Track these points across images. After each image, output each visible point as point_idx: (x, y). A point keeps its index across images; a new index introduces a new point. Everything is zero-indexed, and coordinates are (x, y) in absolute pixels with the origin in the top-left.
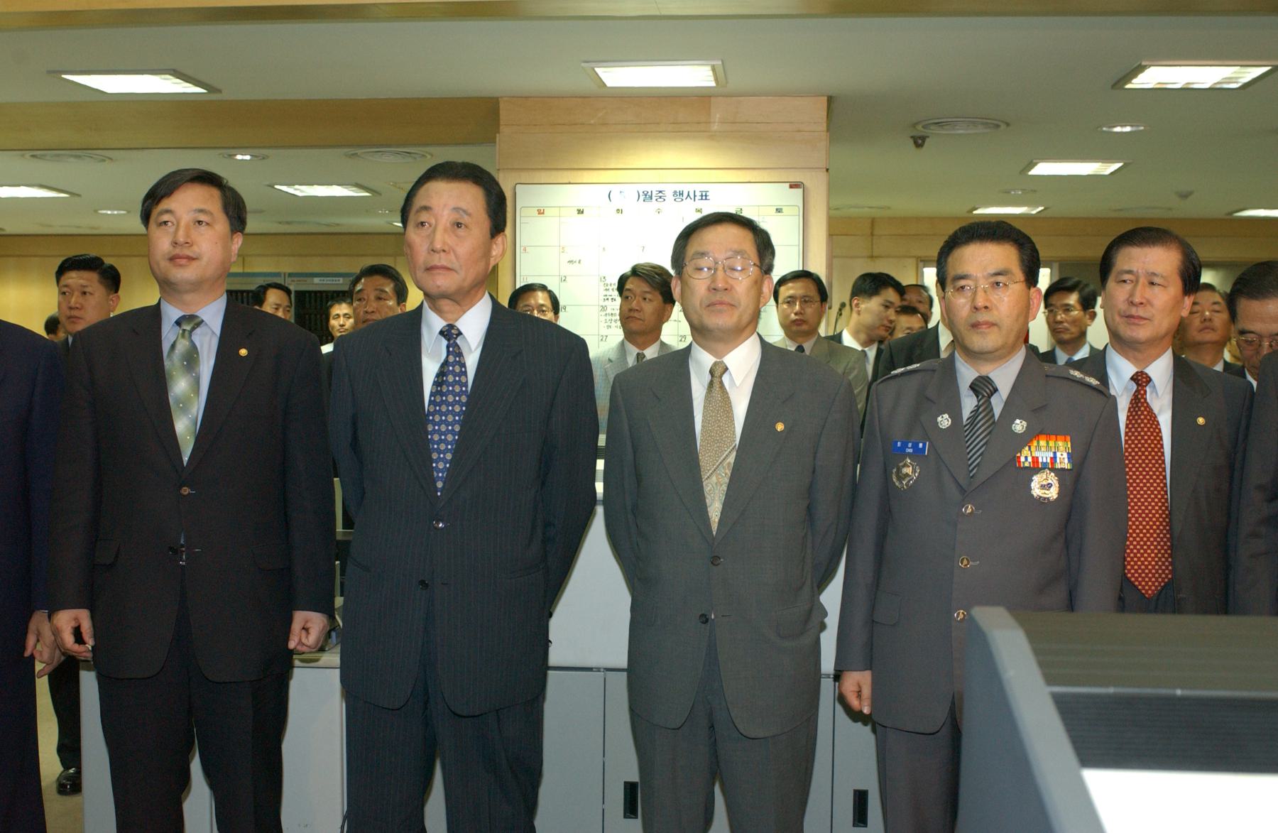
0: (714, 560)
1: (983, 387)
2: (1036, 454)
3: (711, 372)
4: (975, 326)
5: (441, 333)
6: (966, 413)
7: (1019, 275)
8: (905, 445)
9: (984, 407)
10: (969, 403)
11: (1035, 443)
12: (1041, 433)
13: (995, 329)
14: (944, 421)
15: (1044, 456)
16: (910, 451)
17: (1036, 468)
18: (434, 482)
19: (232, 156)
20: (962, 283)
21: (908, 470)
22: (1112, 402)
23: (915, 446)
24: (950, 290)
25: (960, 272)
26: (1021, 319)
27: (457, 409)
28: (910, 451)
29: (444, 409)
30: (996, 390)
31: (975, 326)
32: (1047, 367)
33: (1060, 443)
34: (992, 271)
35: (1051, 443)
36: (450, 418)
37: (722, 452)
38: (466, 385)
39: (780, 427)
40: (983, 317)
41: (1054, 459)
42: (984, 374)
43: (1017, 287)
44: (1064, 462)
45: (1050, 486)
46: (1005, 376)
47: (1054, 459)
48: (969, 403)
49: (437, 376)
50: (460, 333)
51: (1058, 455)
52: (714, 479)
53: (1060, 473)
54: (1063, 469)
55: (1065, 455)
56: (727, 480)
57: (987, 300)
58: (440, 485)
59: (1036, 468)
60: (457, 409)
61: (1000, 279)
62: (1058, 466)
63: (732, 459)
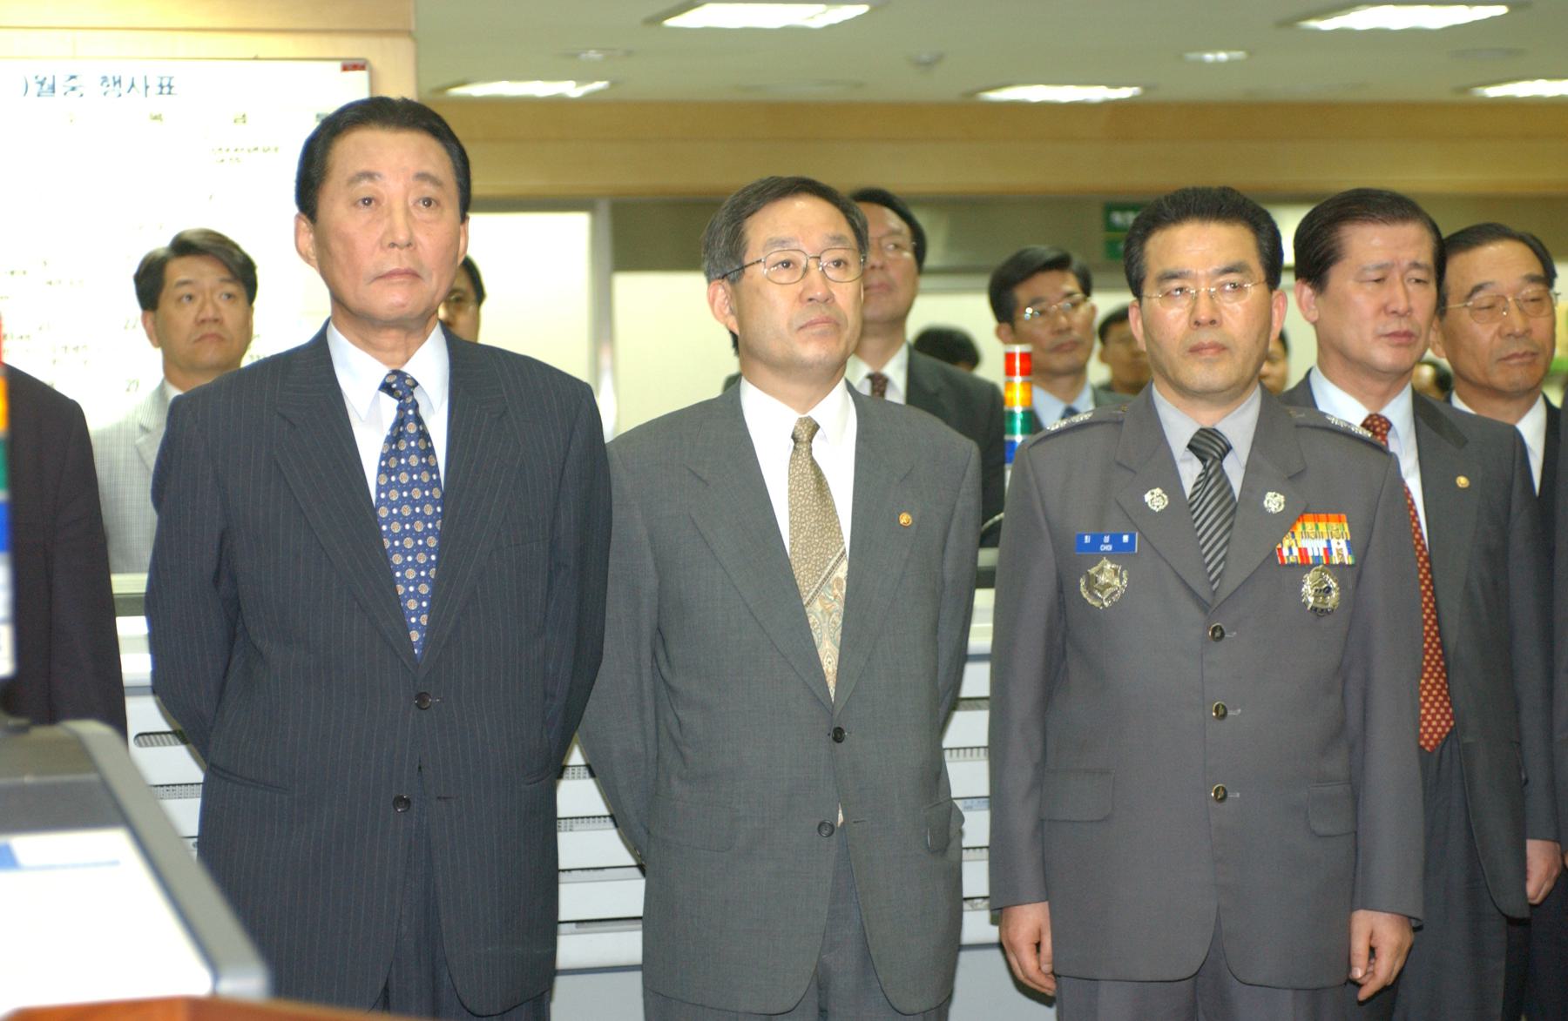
0: (838, 735)
1: (1208, 445)
3: (794, 437)
4: (1196, 350)
5: (386, 387)
6: (1188, 490)
7: (1259, 272)
8: (1097, 540)
9: (1213, 476)
10: (1190, 471)
12: (1306, 511)
13: (1226, 355)
14: (1156, 500)
16: (1109, 548)
18: (406, 629)
19: (613, 84)
20: (1176, 284)
21: (1103, 579)
22: (1392, 461)
23: (1116, 540)
24: (1151, 292)
25: (1171, 265)
26: (1263, 340)
27: (429, 510)
28: (1109, 548)
29: (406, 511)
30: (1229, 448)
31: (1196, 350)
32: (1299, 415)
33: (1334, 526)
34: (1223, 266)
36: (419, 526)
37: (825, 563)
38: (435, 470)
39: (905, 519)
40: (1207, 336)
41: (1328, 550)
42: (1207, 425)
43: (1254, 291)
44: (1342, 553)
45: (1328, 590)
46: (1239, 425)
47: (1328, 550)
48: (1190, 471)
49: (384, 457)
50: (416, 384)
51: (1334, 542)
52: (817, 606)
54: (1342, 565)
56: (839, 606)
57: (1215, 309)
58: (415, 636)
60: (429, 510)
61: (1234, 277)
63: (842, 571)
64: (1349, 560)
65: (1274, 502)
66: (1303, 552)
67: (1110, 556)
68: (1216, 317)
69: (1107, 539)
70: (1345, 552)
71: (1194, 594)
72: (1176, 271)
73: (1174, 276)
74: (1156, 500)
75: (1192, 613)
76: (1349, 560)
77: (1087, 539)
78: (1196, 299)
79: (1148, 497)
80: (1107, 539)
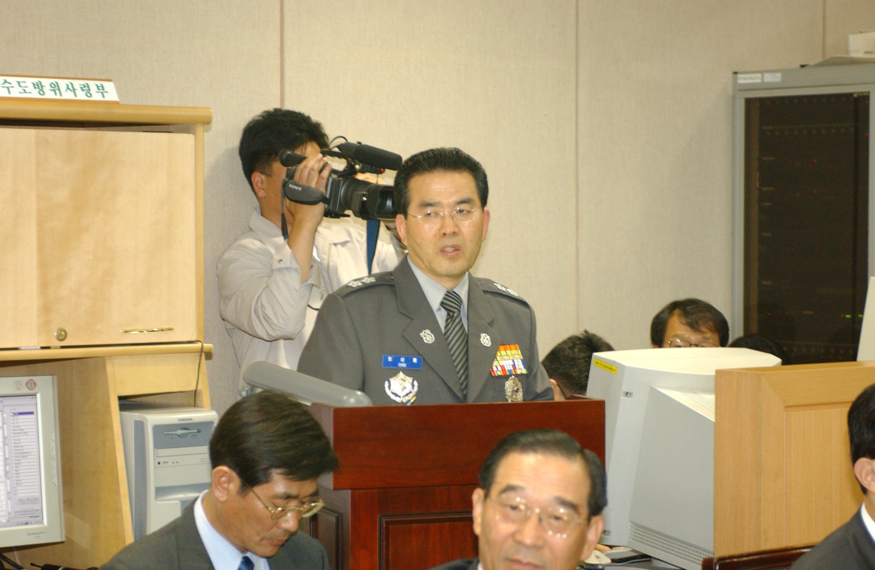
2: (502, 363)
8: (396, 361)
11: (499, 354)
14: (428, 337)
15: (508, 365)
16: (404, 365)
17: (506, 377)
23: (408, 361)
28: (404, 365)
33: (514, 352)
35: (509, 352)
41: (514, 366)
45: (517, 391)
51: (516, 361)
54: (522, 375)
55: (520, 362)
57: (456, 226)
59: (506, 377)
61: (464, 207)
62: (519, 372)
64: (524, 371)
65: (485, 340)
66: (503, 368)
67: (407, 372)
68: (456, 230)
69: (403, 360)
70: (522, 366)
72: (431, 202)
73: (430, 205)
74: (428, 337)
76: (524, 371)
77: (390, 359)
78: (443, 218)
79: (422, 334)
80: (403, 360)
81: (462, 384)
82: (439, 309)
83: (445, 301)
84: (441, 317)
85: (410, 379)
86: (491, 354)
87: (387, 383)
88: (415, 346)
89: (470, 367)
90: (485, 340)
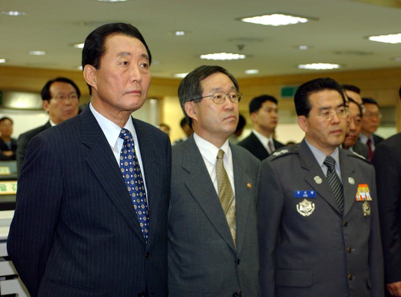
8: (302, 193)
16: (306, 196)
17: (363, 202)
23: (309, 193)
28: (306, 196)
41: (366, 196)
53: (369, 202)
62: (368, 199)
64: (371, 199)
65: (351, 181)
66: (361, 196)
69: (305, 193)
70: (370, 196)
71: (335, 210)
74: (318, 180)
75: (337, 218)
76: (371, 199)
79: (315, 179)
80: (305, 193)
81: (340, 206)
82: (323, 166)
83: (326, 162)
84: (325, 170)
85: (309, 203)
86: (354, 189)
87: (297, 206)
88: (312, 185)
89: (345, 196)
90: (351, 181)
